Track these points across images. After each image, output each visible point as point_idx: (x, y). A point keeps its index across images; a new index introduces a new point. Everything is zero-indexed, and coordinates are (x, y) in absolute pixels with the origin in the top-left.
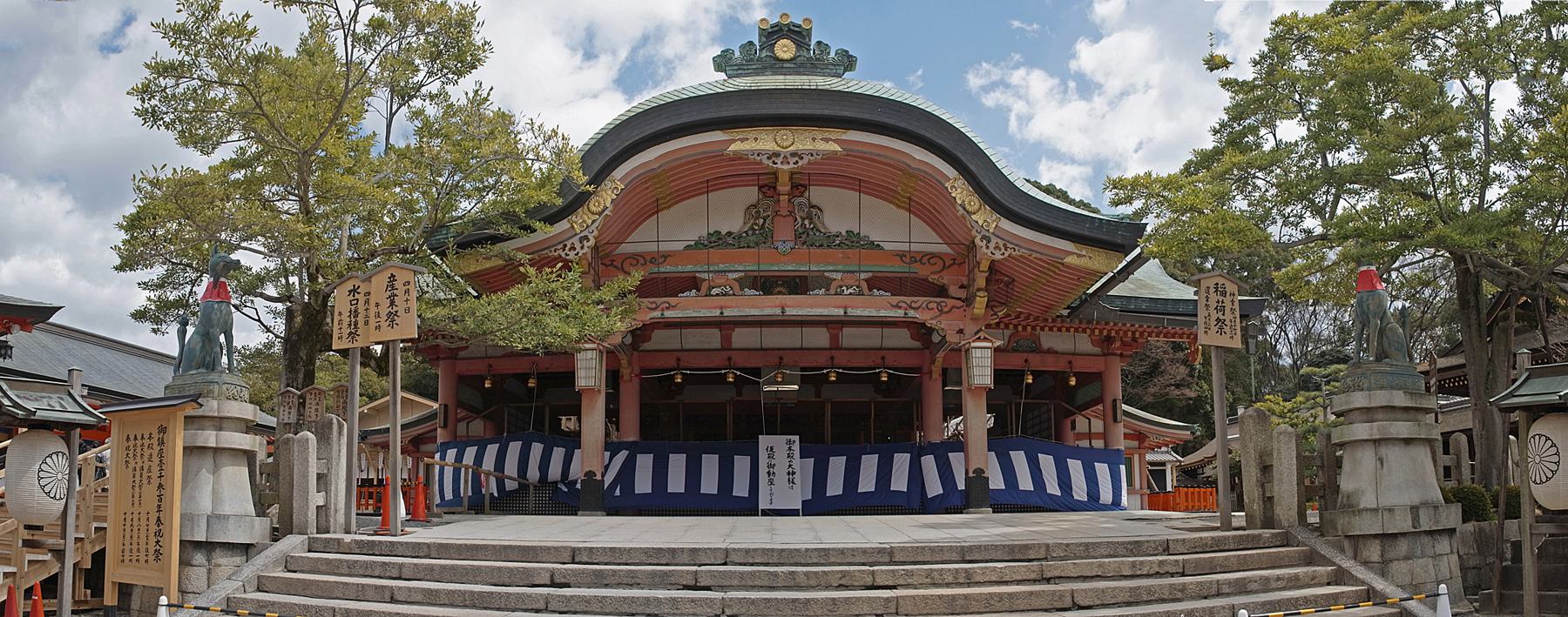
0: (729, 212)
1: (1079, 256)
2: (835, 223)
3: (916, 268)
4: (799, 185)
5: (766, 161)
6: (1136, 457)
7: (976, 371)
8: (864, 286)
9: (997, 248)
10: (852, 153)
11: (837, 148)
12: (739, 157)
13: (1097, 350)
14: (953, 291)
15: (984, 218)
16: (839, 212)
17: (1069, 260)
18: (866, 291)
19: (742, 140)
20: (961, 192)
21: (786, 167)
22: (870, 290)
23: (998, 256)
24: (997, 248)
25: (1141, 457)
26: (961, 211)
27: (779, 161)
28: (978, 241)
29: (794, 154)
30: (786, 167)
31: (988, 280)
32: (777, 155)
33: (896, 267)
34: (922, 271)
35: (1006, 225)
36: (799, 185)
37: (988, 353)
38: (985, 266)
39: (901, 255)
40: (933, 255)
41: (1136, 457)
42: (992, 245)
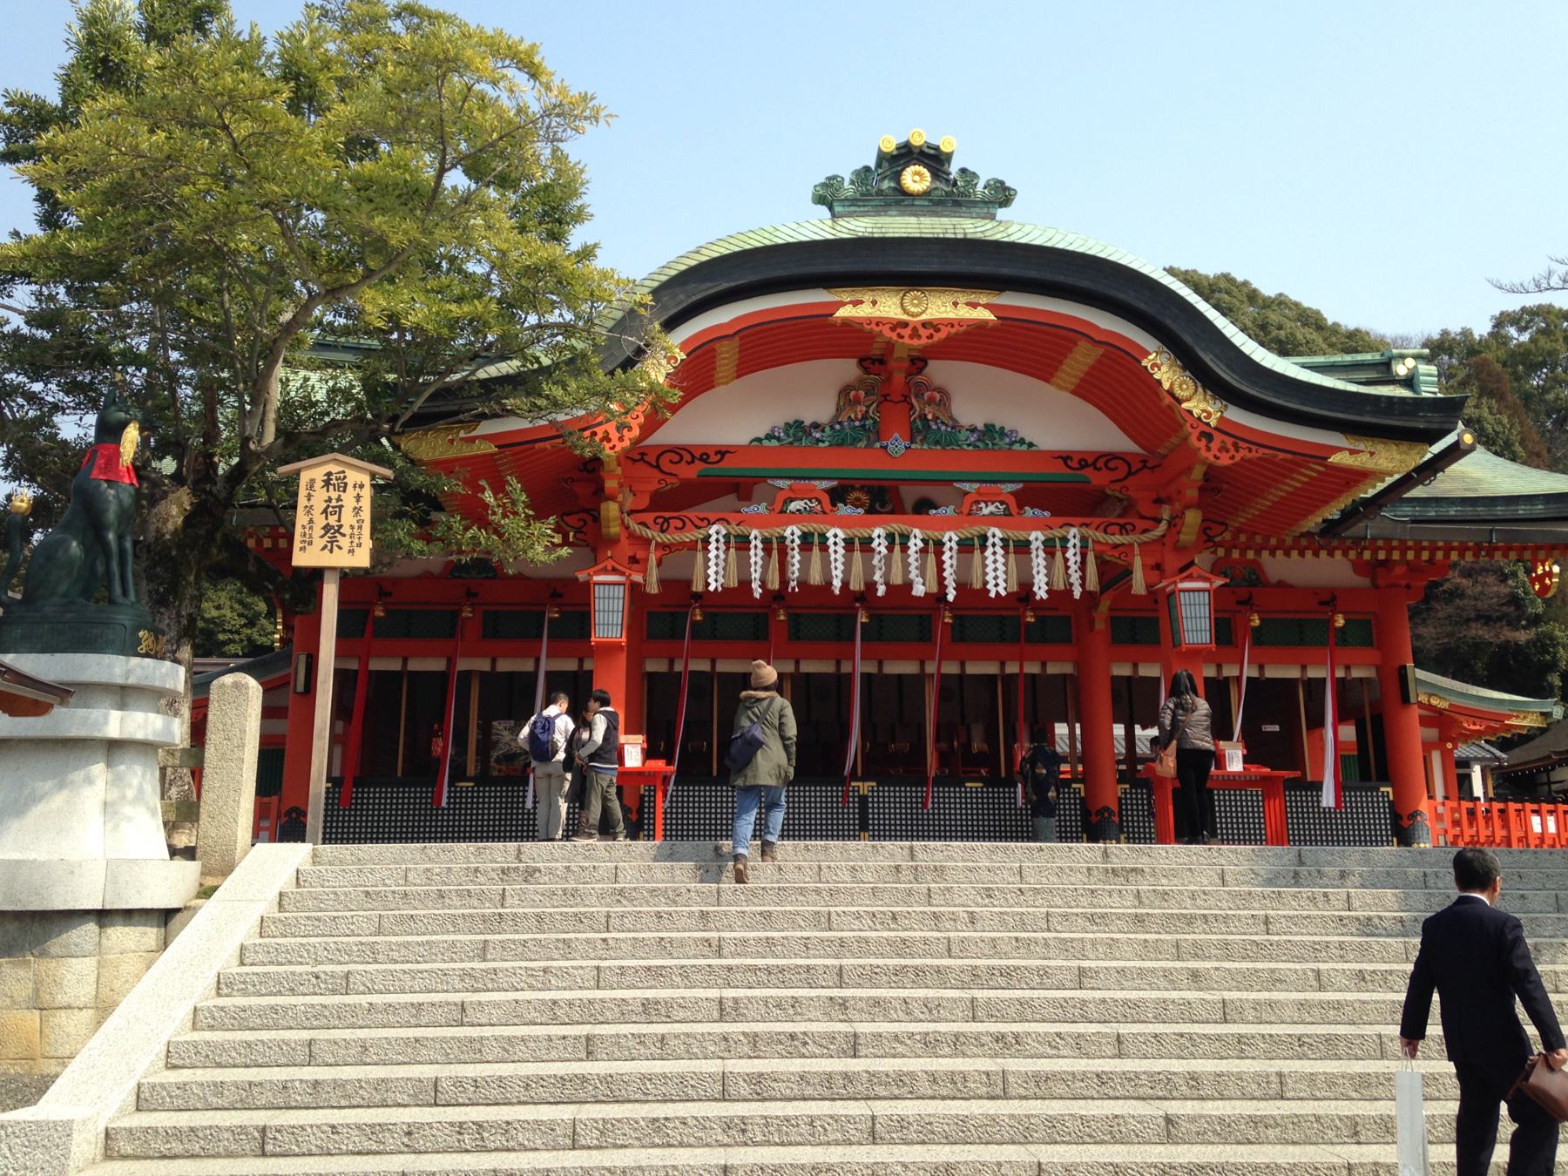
0: (812, 393)
1: (1352, 452)
2: (969, 412)
3: (1088, 473)
4: (918, 362)
5: (888, 333)
6: (1436, 757)
7: (1187, 624)
8: (1012, 502)
9: (1223, 449)
10: (1009, 322)
11: (987, 315)
12: (847, 323)
13: (1363, 582)
14: (1145, 507)
15: (1200, 405)
16: (978, 398)
17: (1335, 459)
18: (1014, 509)
19: (856, 303)
20: (1166, 373)
21: (915, 342)
22: (1020, 507)
23: (1224, 460)
24: (1223, 449)
25: (1446, 755)
26: (1168, 400)
27: (906, 332)
28: (1193, 440)
29: (925, 324)
30: (915, 342)
31: (1201, 489)
32: (905, 324)
33: (1060, 471)
34: (1096, 479)
35: (1236, 415)
36: (918, 362)
37: (1204, 598)
38: (1198, 473)
39: (1065, 458)
40: (1110, 457)
41: (1436, 757)
42: (1215, 445)
